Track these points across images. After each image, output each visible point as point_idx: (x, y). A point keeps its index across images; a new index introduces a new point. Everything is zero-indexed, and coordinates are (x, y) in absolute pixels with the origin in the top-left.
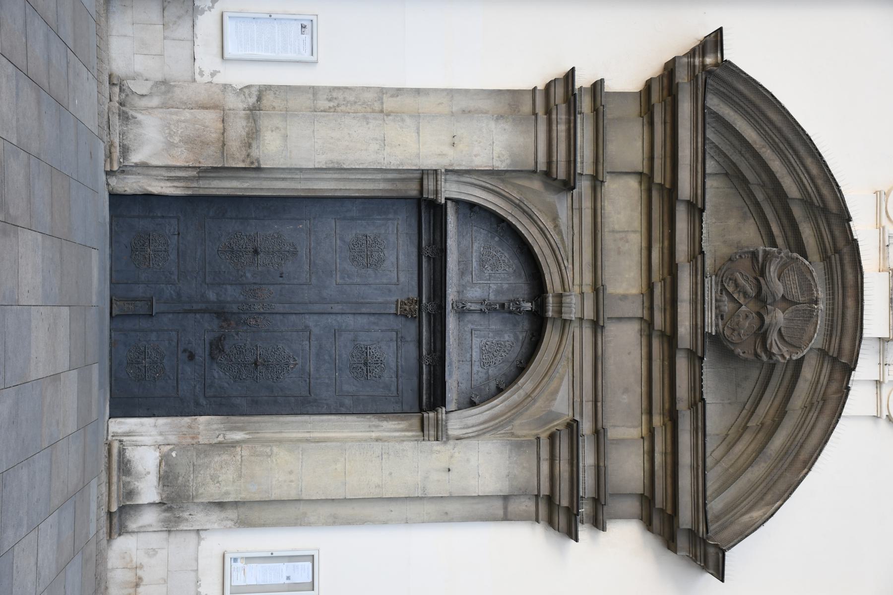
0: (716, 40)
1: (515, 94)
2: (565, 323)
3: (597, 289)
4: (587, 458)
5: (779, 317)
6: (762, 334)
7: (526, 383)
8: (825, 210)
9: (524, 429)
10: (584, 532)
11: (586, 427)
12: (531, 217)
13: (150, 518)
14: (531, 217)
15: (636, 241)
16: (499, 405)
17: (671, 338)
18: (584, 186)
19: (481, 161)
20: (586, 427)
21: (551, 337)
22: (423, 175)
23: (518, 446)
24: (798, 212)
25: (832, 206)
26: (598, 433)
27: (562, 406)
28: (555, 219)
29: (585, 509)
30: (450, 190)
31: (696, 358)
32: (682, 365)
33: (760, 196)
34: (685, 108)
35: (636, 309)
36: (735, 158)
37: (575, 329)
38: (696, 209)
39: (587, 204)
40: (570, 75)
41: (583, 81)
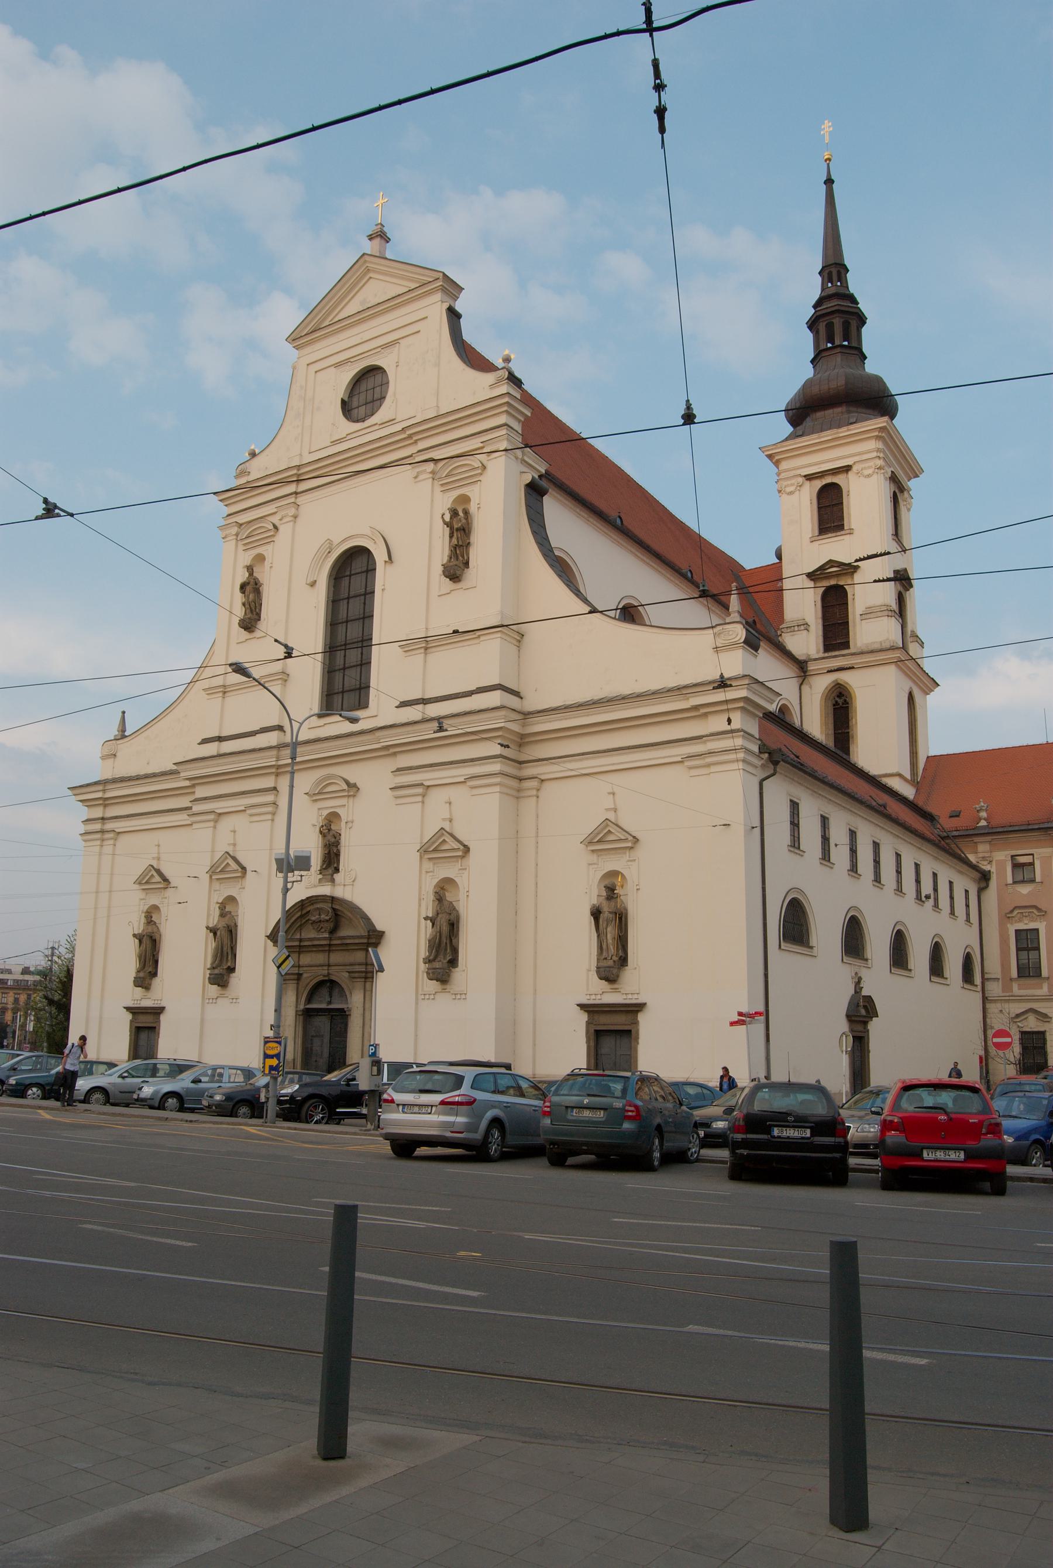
2: (329, 974)
4: (357, 968)
5: (323, 916)
6: (327, 921)
8: (302, 905)
12: (308, 984)
14: (308, 984)
19: (294, 998)
24: (304, 912)
25: (300, 904)
28: (308, 977)
33: (304, 921)
36: (295, 929)
37: (330, 972)
39: (305, 969)
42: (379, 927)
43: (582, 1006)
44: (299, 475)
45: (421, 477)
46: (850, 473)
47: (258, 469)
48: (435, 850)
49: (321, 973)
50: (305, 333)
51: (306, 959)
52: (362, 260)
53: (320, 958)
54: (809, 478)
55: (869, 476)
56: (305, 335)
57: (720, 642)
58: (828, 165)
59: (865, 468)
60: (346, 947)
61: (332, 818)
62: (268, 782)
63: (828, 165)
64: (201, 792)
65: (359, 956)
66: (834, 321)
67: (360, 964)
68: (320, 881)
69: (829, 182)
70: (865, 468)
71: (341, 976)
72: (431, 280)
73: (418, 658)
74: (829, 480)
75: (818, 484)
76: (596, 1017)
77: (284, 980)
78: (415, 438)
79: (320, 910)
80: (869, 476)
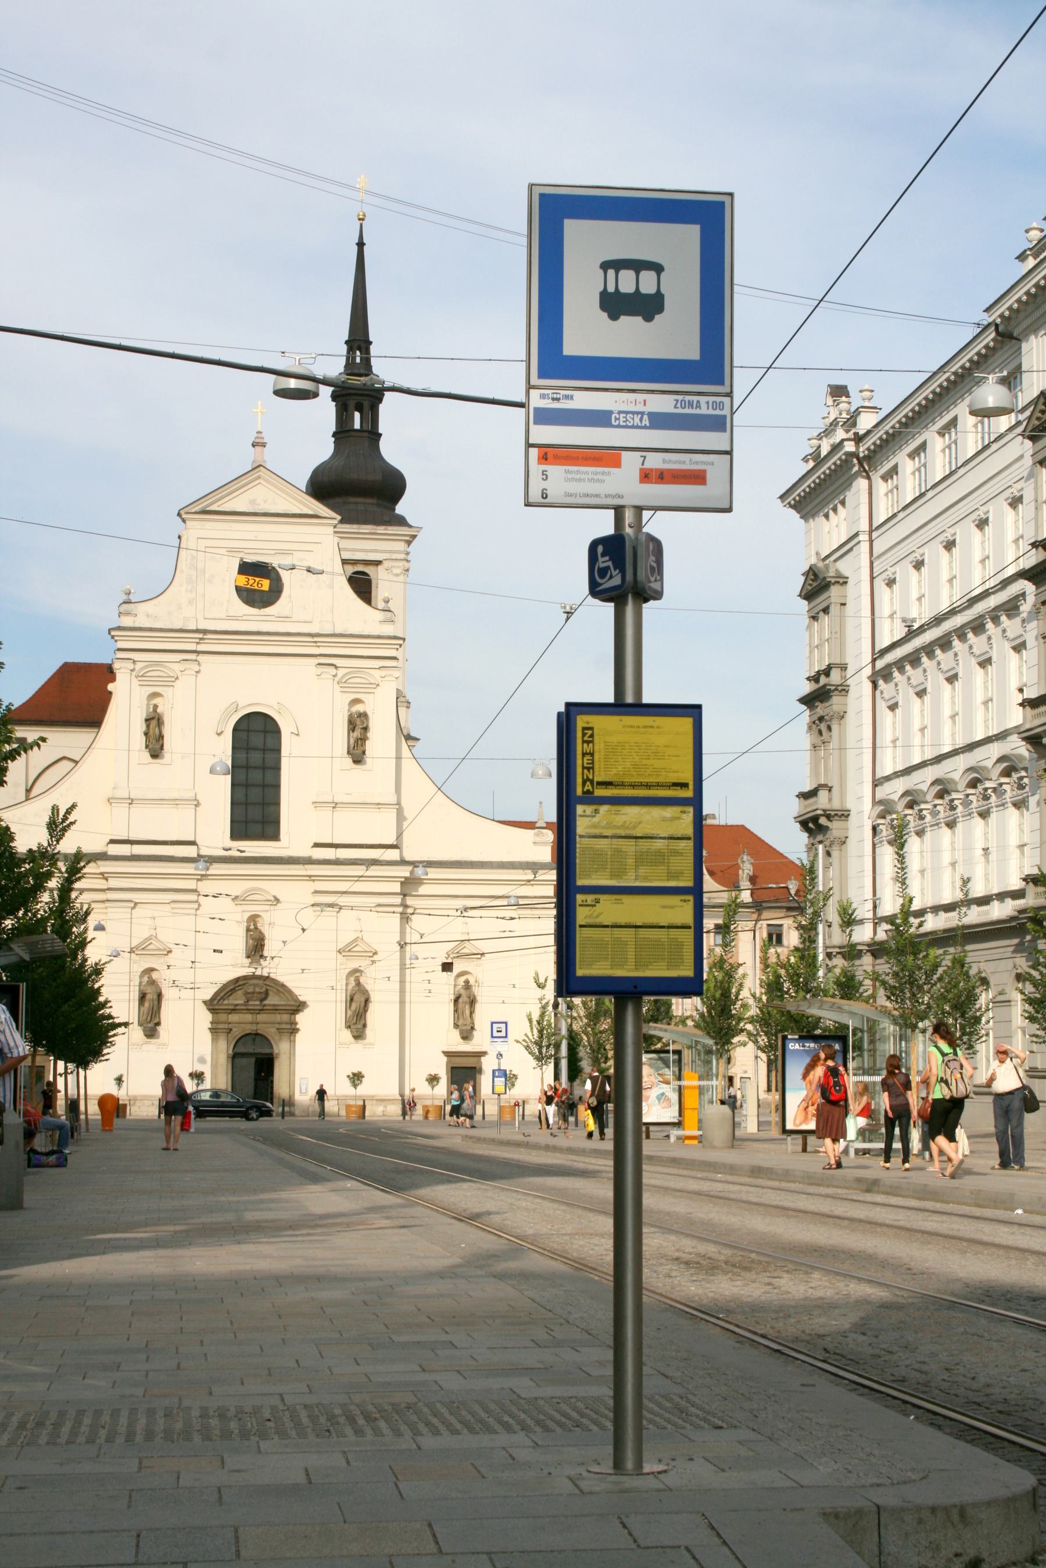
0: (205, 1002)
1: (212, 1039)
3: (251, 1023)
4: (284, 1026)
5: (257, 990)
6: (260, 993)
7: (269, 1037)
9: (277, 1037)
10: (298, 1026)
11: (277, 1026)
13: (292, 1109)
15: (241, 1015)
16: (273, 1043)
17: (261, 1010)
18: (230, 1026)
19: (226, 1046)
20: (277, 1026)
21: (259, 1032)
22: (228, 1057)
23: (280, 1039)
26: (279, 1023)
27: (273, 1030)
29: (293, 1027)
30: (231, 1052)
31: (265, 1005)
32: (265, 1008)
34: (217, 1007)
35: (255, 1015)
38: (237, 1005)
40: (210, 1029)
41: (210, 1026)
42: (301, 999)
43: (444, 1052)
44: (201, 639)
45: (323, 676)
46: (379, 567)
47: (143, 616)
48: (349, 951)
49: (249, 1029)
50: (193, 511)
51: (223, 1017)
52: (257, 470)
53: (249, 1017)
54: (345, 562)
55: (397, 575)
56: (196, 513)
57: (538, 839)
58: (361, 225)
59: (394, 567)
60: (275, 1009)
61: (254, 918)
62: (191, 884)
63: (361, 225)
64: (113, 883)
65: (286, 1017)
66: (364, 403)
67: (286, 1023)
68: (250, 963)
69: (361, 245)
70: (394, 567)
71: (270, 1032)
72: (327, 516)
73: (328, 812)
74: (360, 568)
75: (350, 569)
76: (453, 1058)
77: (214, 1030)
78: (318, 644)
79: (255, 985)
80: (397, 575)
